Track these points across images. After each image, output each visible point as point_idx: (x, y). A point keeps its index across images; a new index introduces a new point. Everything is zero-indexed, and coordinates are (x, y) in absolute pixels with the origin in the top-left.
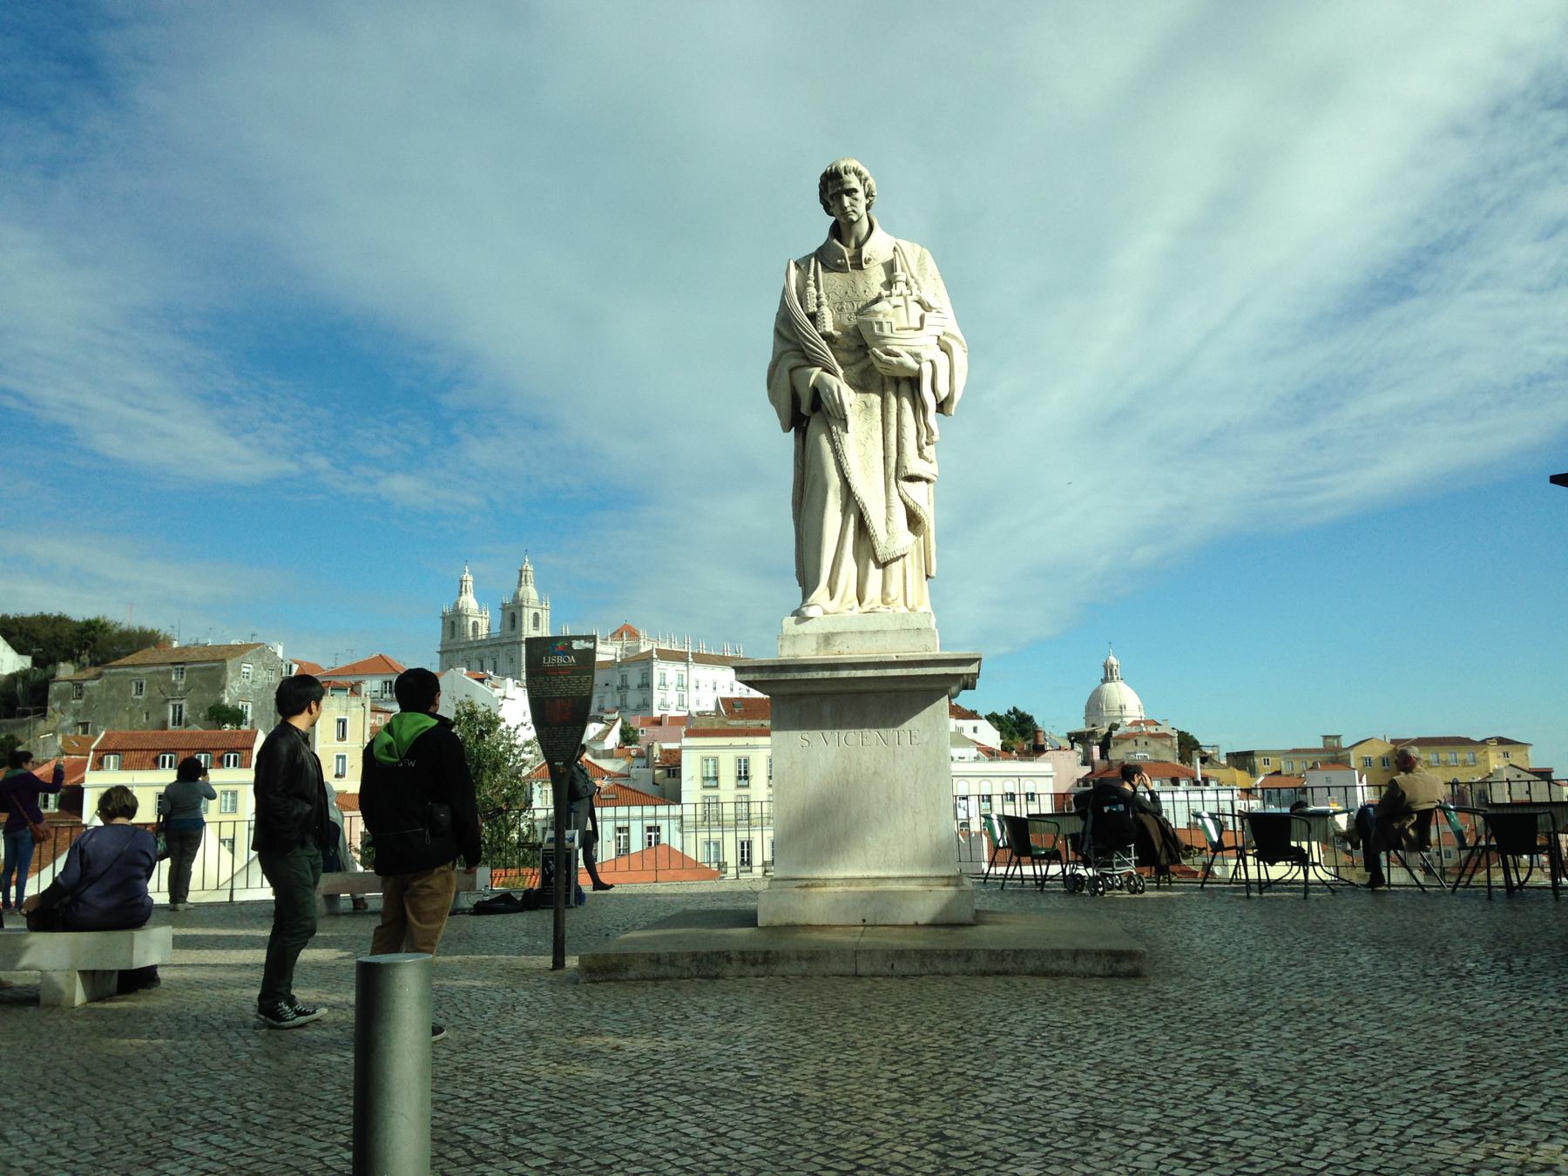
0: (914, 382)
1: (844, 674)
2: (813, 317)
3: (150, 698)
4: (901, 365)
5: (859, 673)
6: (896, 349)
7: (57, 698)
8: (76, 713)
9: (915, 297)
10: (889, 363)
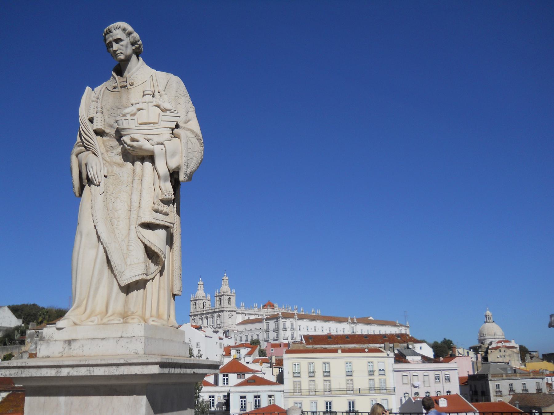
0: (151, 158)
1: (64, 372)
2: (91, 120)
4: (140, 148)
5: (74, 372)
6: (136, 137)
7: (29, 337)
9: (155, 103)
10: (132, 147)
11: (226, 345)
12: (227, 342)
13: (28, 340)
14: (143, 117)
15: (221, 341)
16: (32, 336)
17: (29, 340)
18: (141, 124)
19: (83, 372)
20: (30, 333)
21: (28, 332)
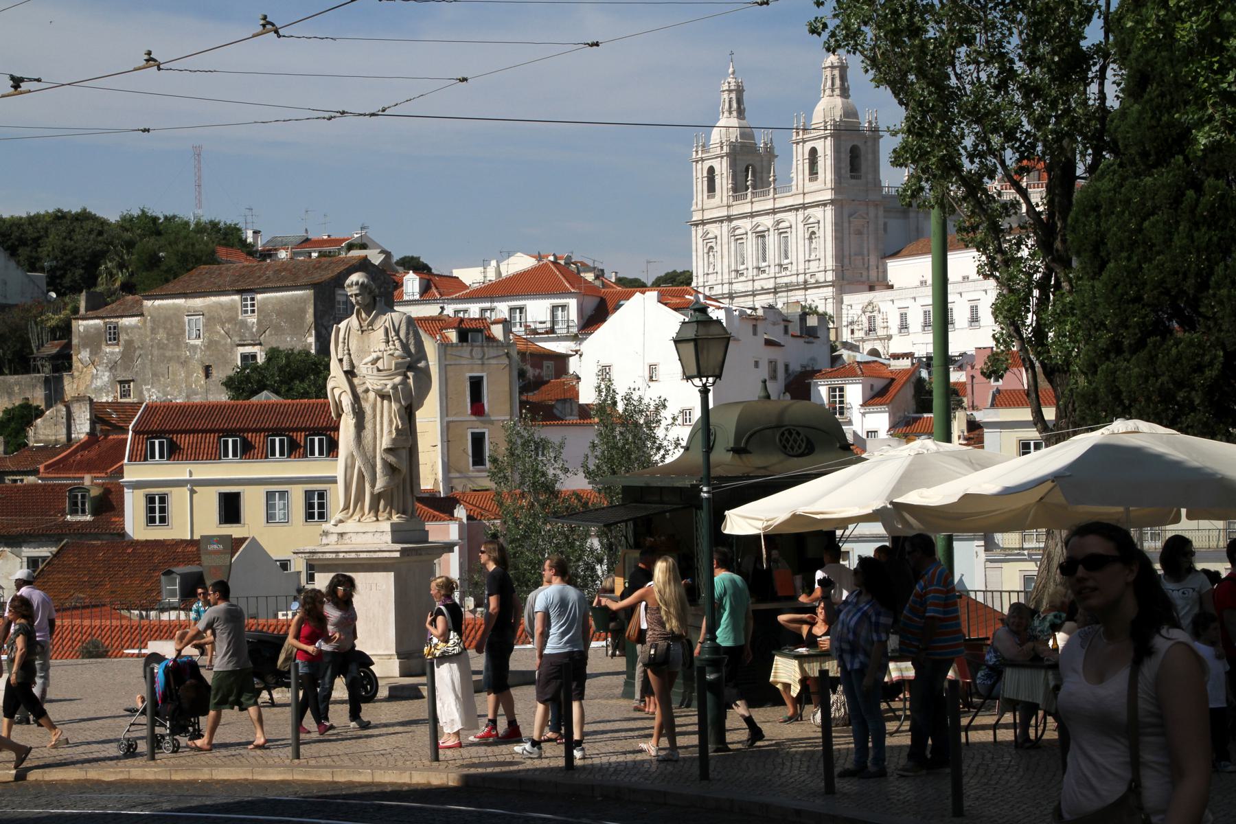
1: (341, 555)
2: (341, 360)
3: (211, 344)
5: (347, 556)
7: (85, 345)
8: (113, 367)
11: (795, 367)
12: (796, 354)
13: (81, 356)
14: (380, 364)
15: (772, 353)
16: (93, 342)
17: (85, 355)
18: (379, 370)
19: (353, 555)
20: (86, 327)
21: (80, 326)
